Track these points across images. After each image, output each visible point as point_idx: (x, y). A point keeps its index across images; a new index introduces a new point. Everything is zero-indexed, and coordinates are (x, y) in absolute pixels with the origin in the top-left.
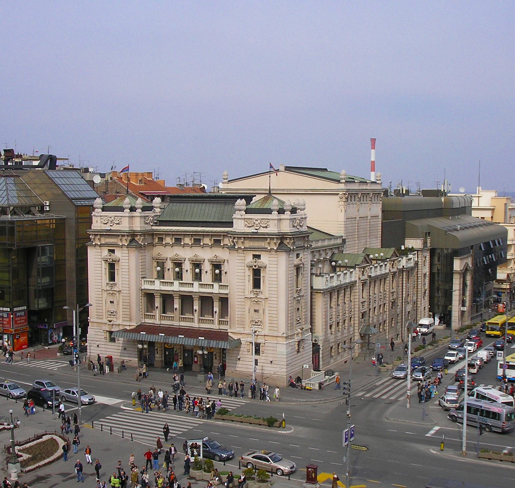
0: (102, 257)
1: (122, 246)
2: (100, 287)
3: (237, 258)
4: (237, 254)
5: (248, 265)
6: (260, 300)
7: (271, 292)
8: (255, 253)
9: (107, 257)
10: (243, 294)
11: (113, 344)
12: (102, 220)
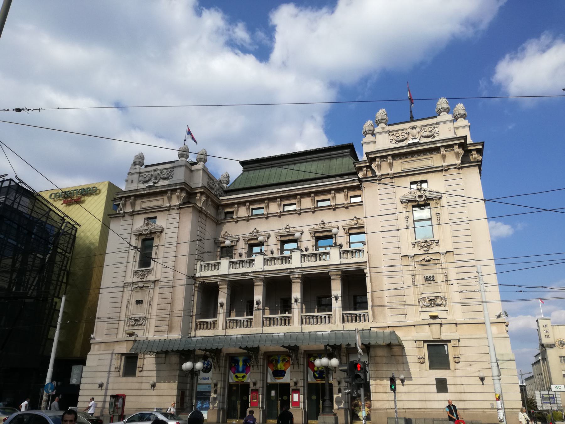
0: (134, 229)
1: (169, 209)
2: (122, 279)
3: (379, 192)
4: (379, 187)
5: (405, 199)
6: (434, 257)
7: (456, 239)
8: (414, 179)
9: (142, 229)
10: (397, 251)
11: (130, 379)
12: (141, 178)
